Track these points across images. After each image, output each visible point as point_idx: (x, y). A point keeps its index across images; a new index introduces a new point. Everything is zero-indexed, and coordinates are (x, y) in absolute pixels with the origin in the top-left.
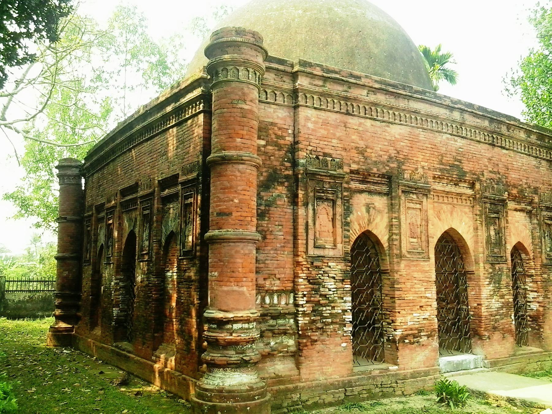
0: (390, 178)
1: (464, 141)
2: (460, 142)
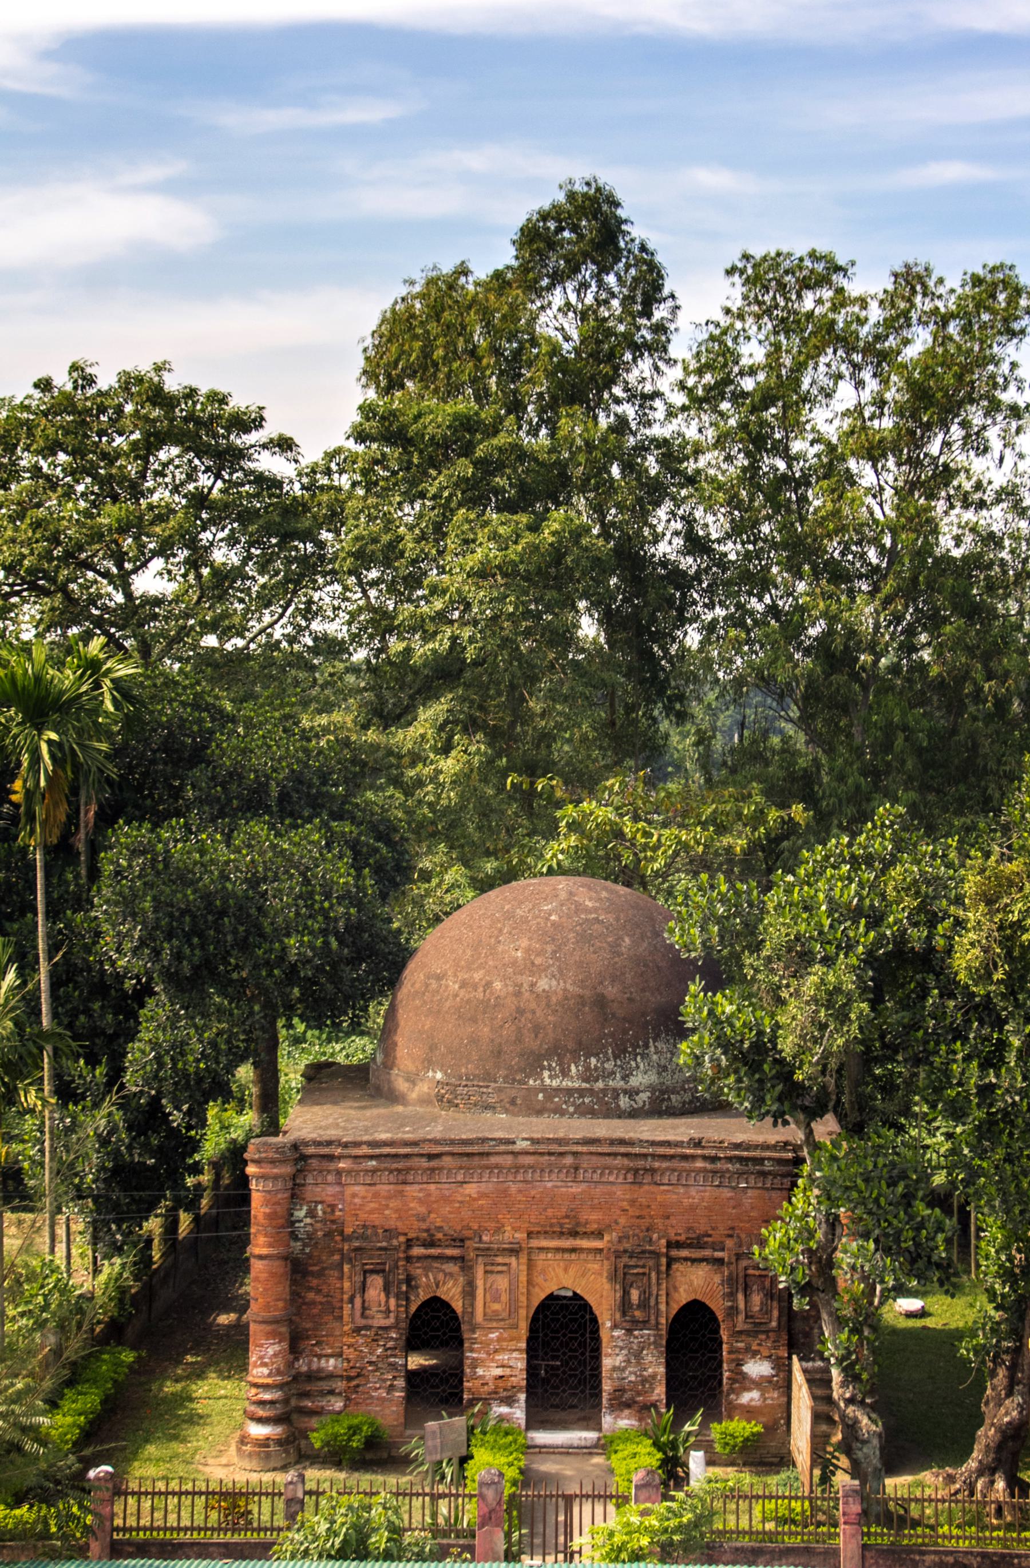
0: (462, 1240)
1: (584, 1186)
2: (576, 1189)
